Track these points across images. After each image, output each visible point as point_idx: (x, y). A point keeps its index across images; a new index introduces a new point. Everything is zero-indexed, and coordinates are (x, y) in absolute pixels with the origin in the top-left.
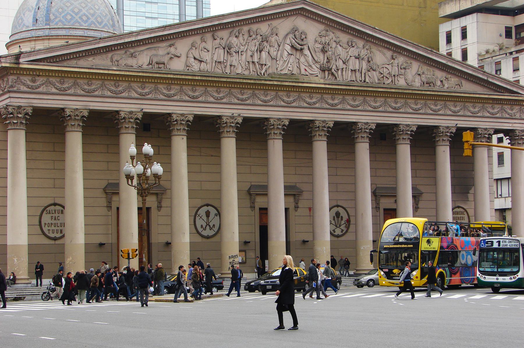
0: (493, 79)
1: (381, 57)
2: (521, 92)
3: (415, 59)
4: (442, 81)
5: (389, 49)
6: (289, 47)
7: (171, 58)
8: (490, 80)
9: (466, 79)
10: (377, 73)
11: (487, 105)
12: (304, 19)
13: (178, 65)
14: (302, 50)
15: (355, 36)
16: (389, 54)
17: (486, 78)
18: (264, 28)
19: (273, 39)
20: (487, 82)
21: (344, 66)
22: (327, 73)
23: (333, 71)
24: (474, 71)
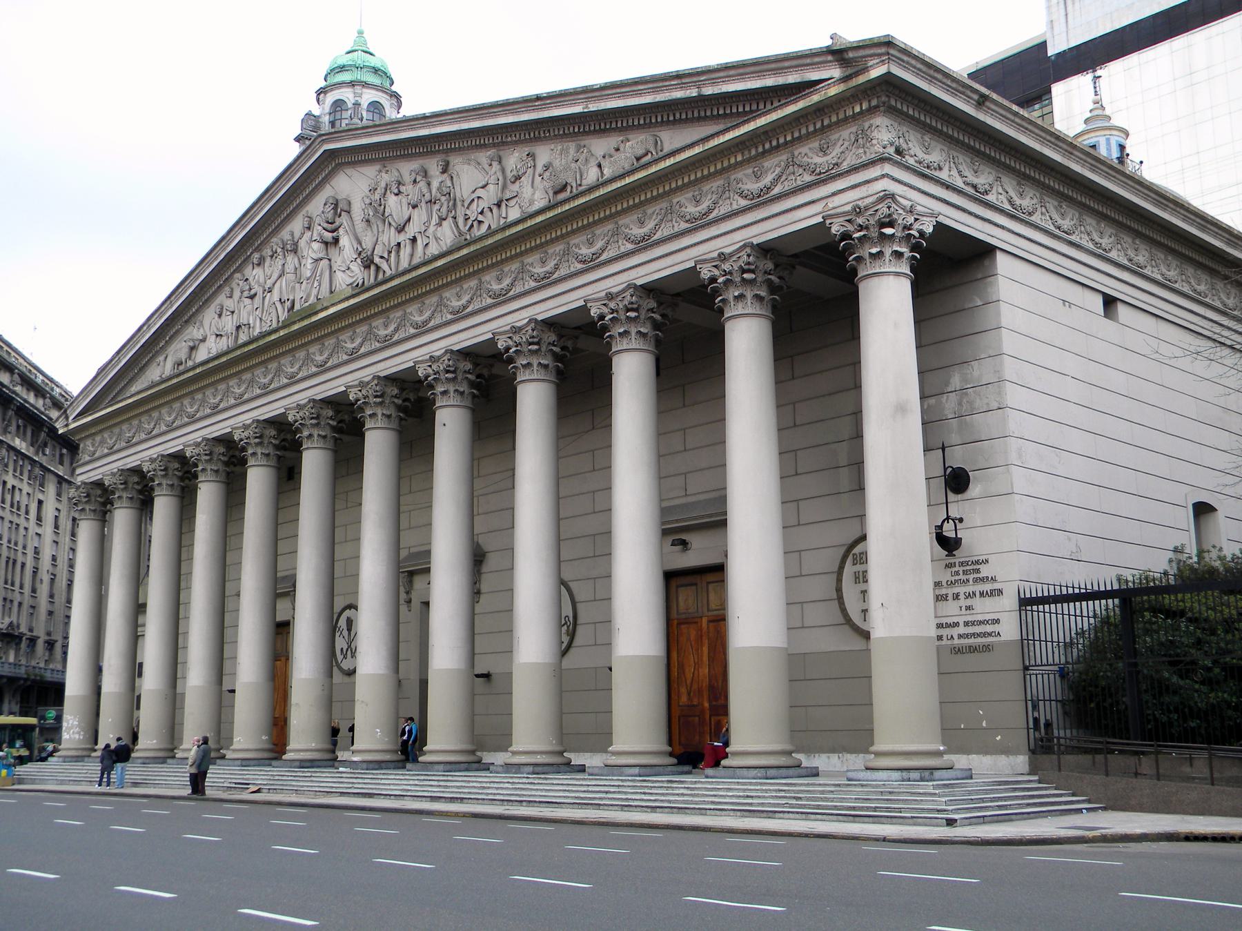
0: (714, 82)
1: (471, 176)
2: (814, 76)
3: (537, 140)
4: (600, 166)
5: (483, 146)
6: (316, 246)
7: (192, 349)
8: (708, 91)
9: (666, 123)
10: (461, 221)
11: (739, 175)
12: (349, 171)
13: (202, 355)
14: (336, 241)
15: (420, 155)
16: (483, 156)
17: (693, 93)
18: (297, 225)
19: (302, 243)
20: (702, 101)
21: (401, 238)
22: (373, 268)
23: (377, 260)
24: (655, 90)
